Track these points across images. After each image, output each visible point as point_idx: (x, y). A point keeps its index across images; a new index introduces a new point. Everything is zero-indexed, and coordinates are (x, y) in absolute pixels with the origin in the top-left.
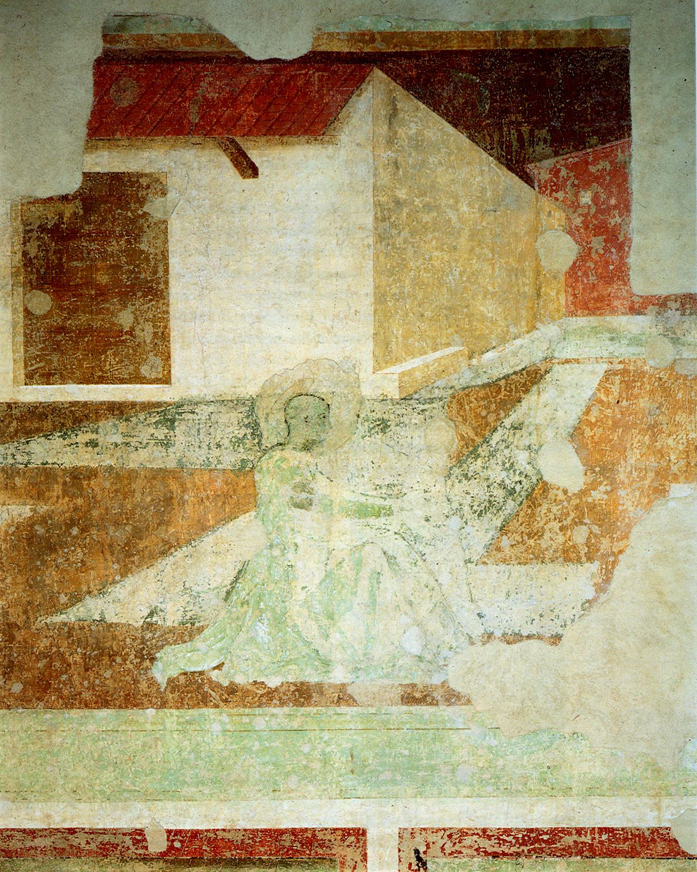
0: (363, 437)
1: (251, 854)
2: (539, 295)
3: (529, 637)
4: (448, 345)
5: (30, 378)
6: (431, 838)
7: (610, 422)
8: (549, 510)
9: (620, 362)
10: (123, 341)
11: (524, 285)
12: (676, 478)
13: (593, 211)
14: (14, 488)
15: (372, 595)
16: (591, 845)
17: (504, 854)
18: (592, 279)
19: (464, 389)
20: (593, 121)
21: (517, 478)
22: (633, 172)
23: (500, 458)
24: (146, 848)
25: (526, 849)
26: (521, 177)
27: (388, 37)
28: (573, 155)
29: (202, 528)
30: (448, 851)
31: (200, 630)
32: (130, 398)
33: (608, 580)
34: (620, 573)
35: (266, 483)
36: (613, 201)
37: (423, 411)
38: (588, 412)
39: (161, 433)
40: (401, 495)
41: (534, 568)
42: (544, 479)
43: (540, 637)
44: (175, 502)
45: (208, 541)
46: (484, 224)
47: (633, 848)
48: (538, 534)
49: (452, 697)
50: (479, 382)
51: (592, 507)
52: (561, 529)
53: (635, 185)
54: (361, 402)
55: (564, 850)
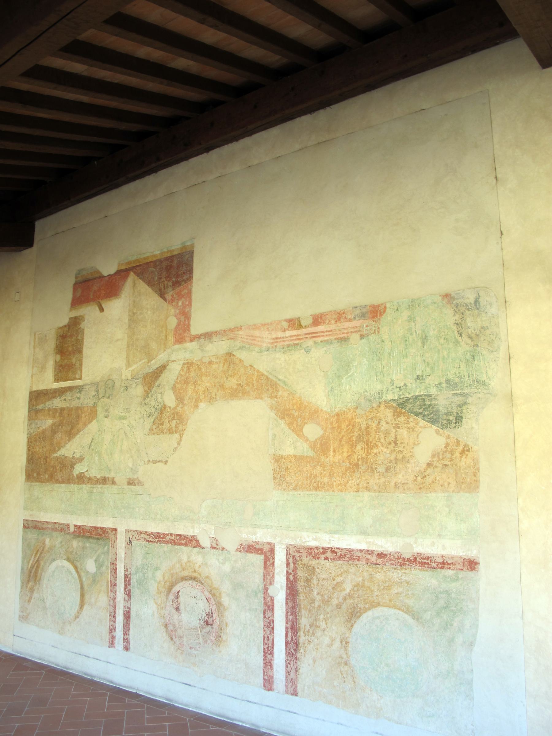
0: (122, 393)
2: (166, 339)
3: (159, 461)
4: (143, 359)
7: (183, 382)
8: (166, 415)
9: (187, 360)
10: (73, 367)
11: (163, 336)
12: (201, 401)
13: (182, 307)
14: (49, 415)
15: (121, 446)
17: (151, 541)
18: (181, 331)
19: (146, 374)
20: (183, 276)
21: (158, 404)
22: (193, 292)
23: (154, 397)
24: (69, 530)
25: (156, 540)
26: (163, 299)
27: (134, 261)
28: (178, 289)
29: (85, 425)
30: (137, 539)
31: (83, 459)
32: (73, 385)
33: (181, 440)
35: (99, 409)
36: (187, 303)
37: (136, 382)
38: (177, 379)
39: (78, 395)
40: (130, 411)
41: (162, 436)
42: (165, 404)
44: (80, 417)
45: (86, 430)
46: (154, 317)
47: (186, 543)
48: (162, 424)
49: (140, 483)
50: (150, 371)
51: (177, 413)
52: (169, 421)
53: (193, 296)
54: (122, 381)
55: (166, 541)
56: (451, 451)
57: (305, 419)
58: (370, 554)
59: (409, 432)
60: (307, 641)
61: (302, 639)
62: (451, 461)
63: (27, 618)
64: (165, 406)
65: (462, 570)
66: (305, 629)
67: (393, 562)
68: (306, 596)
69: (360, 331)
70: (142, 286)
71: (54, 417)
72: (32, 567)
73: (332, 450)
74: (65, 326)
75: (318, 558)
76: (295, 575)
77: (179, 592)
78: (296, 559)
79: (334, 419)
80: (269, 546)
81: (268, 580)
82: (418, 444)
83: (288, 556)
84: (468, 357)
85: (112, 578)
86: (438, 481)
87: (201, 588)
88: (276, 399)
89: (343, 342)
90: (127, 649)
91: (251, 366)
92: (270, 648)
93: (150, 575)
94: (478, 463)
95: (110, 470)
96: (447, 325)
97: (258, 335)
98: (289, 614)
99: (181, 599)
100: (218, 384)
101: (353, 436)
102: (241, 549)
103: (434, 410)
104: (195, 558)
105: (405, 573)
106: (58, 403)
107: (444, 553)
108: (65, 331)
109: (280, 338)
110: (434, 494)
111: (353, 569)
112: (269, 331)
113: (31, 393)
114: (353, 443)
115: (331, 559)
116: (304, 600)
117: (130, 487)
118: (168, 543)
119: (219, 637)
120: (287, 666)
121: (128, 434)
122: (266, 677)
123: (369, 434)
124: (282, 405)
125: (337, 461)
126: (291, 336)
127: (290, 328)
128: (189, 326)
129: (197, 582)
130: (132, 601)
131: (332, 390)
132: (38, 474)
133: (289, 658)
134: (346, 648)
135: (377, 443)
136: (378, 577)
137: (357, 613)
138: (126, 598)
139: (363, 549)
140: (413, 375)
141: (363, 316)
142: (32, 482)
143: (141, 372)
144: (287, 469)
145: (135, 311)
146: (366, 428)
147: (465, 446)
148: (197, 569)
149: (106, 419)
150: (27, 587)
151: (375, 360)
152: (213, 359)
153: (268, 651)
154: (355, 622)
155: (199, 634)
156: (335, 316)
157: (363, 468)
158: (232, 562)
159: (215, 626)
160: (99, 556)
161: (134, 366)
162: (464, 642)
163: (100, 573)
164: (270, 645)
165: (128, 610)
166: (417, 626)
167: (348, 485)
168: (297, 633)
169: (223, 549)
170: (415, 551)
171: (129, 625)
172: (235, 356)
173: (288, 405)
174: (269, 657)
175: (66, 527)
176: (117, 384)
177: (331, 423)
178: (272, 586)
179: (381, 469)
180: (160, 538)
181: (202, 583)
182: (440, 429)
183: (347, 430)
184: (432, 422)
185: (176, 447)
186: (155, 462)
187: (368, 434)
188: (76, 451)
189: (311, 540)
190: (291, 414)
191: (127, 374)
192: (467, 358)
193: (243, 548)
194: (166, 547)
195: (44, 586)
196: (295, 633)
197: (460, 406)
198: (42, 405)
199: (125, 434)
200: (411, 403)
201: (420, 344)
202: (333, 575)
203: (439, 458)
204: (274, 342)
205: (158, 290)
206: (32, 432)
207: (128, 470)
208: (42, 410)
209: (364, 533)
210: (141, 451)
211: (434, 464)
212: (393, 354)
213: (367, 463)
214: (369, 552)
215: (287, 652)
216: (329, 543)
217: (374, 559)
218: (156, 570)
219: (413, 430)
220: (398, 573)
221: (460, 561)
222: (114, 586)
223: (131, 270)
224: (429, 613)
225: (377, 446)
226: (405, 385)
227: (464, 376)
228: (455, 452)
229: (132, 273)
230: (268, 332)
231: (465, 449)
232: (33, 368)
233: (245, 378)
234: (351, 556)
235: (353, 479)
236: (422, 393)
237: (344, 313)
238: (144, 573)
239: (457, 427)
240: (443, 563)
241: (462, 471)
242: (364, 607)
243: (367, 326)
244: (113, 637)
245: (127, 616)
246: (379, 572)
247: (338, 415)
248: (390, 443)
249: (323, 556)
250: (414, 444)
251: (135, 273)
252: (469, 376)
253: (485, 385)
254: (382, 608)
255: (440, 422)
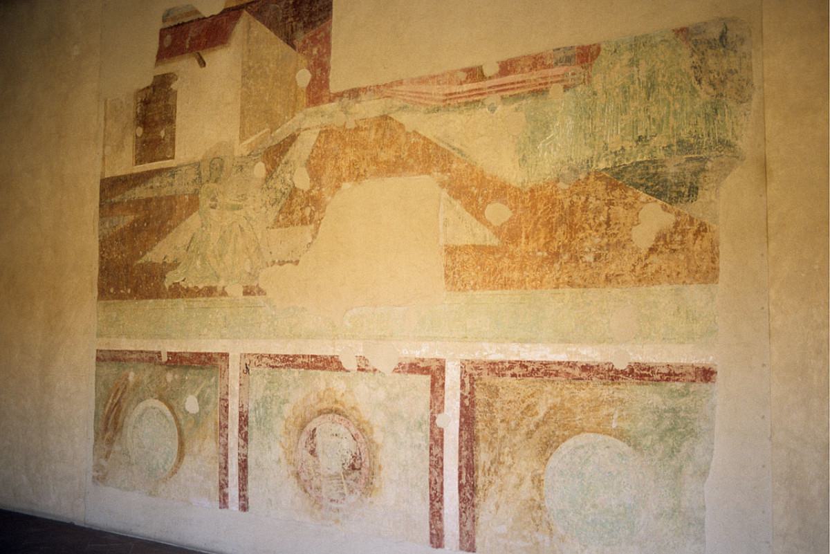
1: (192, 363)
2: (296, 100)
3: (288, 262)
4: (264, 129)
5: (136, 164)
6: (251, 358)
8: (297, 201)
12: (344, 180)
15: (235, 245)
16: (308, 363)
25: (284, 364)
26: (292, 47)
29: (181, 220)
32: (162, 166)
33: (317, 233)
34: (321, 229)
35: (202, 198)
36: (325, 51)
38: (312, 152)
39: (170, 180)
40: (246, 199)
41: (291, 228)
43: (292, 262)
47: (324, 365)
48: (292, 213)
49: (261, 292)
50: (274, 144)
51: (312, 197)
52: (301, 209)
54: (234, 159)
55: (297, 365)
56: (682, 232)
57: (487, 197)
58: (571, 367)
59: (627, 209)
60: (487, 482)
61: (481, 480)
62: (681, 244)
63: (104, 478)
64: (295, 189)
65: (694, 381)
66: (484, 466)
67: (602, 375)
68: (486, 426)
69: (562, 81)
70: (260, 30)
71: (136, 211)
72: (111, 411)
73: (523, 235)
74: (148, 88)
75: (503, 375)
76: (472, 398)
77: (315, 429)
78: (473, 378)
79: (527, 197)
80: (437, 363)
81: (436, 407)
82: (638, 224)
83: (463, 375)
84: (709, 110)
85: (222, 418)
86: (664, 270)
87: (344, 423)
88: (449, 174)
89: (539, 96)
90: (244, 508)
91: (415, 132)
92: (437, 494)
93: (275, 411)
94: (718, 246)
95: (218, 277)
96: (681, 70)
97: (424, 91)
98: (463, 449)
99: (318, 439)
100: (369, 157)
101: (553, 217)
102: (401, 370)
103: (661, 179)
104: (335, 385)
105: (618, 389)
106: (140, 192)
107: (670, 361)
108: (148, 94)
109: (455, 93)
110: (658, 288)
111: (549, 387)
112: (439, 84)
113: (103, 181)
114: (552, 227)
115: (519, 376)
116: (484, 429)
117: (247, 297)
118: (300, 367)
119: (369, 483)
120: (461, 516)
121: (245, 228)
122: (434, 532)
123: (573, 214)
124: (457, 181)
125: (531, 250)
126: (470, 91)
127: (469, 80)
128: (327, 81)
129: (340, 415)
130: (249, 446)
131: (524, 159)
132: (117, 289)
133: (464, 506)
134: (539, 488)
135: (584, 225)
136: (583, 395)
137: (553, 442)
138: (242, 443)
139: (562, 360)
140: (633, 136)
141: (568, 60)
142: (108, 299)
143: (260, 146)
144: (463, 264)
145: (251, 64)
146: (570, 207)
147: (701, 224)
148: (338, 398)
149: (212, 210)
150: (103, 438)
151: (584, 119)
152: (361, 124)
153: (436, 498)
154: (551, 454)
155: (342, 483)
156: (529, 62)
157: (566, 257)
158: (388, 387)
159: (364, 470)
160: (203, 391)
161: (252, 139)
162: (695, 472)
163: (205, 413)
164: (438, 490)
165: (245, 458)
166: (634, 455)
167: (545, 280)
168: (474, 473)
169: (375, 370)
170: (631, 360)
171: (246, 477)
172: (393, 120)
173: (466, 182)
174: (437, 505)
175: (156, 355)
176: (228, 163)
177: (523, 202)
178: (439, 415)
179: (589, 258)
180: (289, 361)
181: (346, 417)
182: (667, 205)
183: (545, 210)
184: (657, 195)
185: (310, 242)
186: (282, 263)
187: (572, 213)
188: (168, 255)
189: (494, 352)
190: (469, 192)
191: (241, 149)
192: (707, 111)
193: (403, 368)
194: (296, 373)
195: (129, 435)
196: (472, 473)
197: (695, 174)
198: (119, 197)
199: (242, 229)
200: (630, 172)
201: (643, 95)
202: (522, 395)
203: (665, 241)
204: (446, 100)
205: (283, 35)
206: (105, 232)
207: (245, 276)
208: (119, 203)
209: (565, 340)
210: (262, 250)
211: (659, 249)
212: (608, 110)
213: (569, 251)
214: (570, 365)
215: (460, 497)
216: (518, 355)
217: (577, 372)
218: (284, 403)
219: (632, 206)
220: (609, 389)
221: (691, 370)
222: (224, 428)
223: (243, 8)
224: (650, 437)
225: (584, 228)
226: (623, 149)
227: (702, 135)
228: (688, 233)
229: (245, 12)
230: (438, 86)
231: (701, 229)
232: (104, 146)
233: (406, 148)
234: (546, 370)
235: (551, 272)
236: (645, 158)
237: (541, 57)
238: (267, 408)
239: (690, 201)
240: (669, 374)
241: (696, 257)
242: (563, 435)
243: (573, 74)
244: (225, 495)
245: (243, 466)
246: (584, 389)
247: (532, 191)
248: (600, 225)
249: (509, 373)
250: (633, 224)
251: (250, 12)
252: (709, 136)
253: (730, 146)
254: (588, 434)
255: (668, 196)
